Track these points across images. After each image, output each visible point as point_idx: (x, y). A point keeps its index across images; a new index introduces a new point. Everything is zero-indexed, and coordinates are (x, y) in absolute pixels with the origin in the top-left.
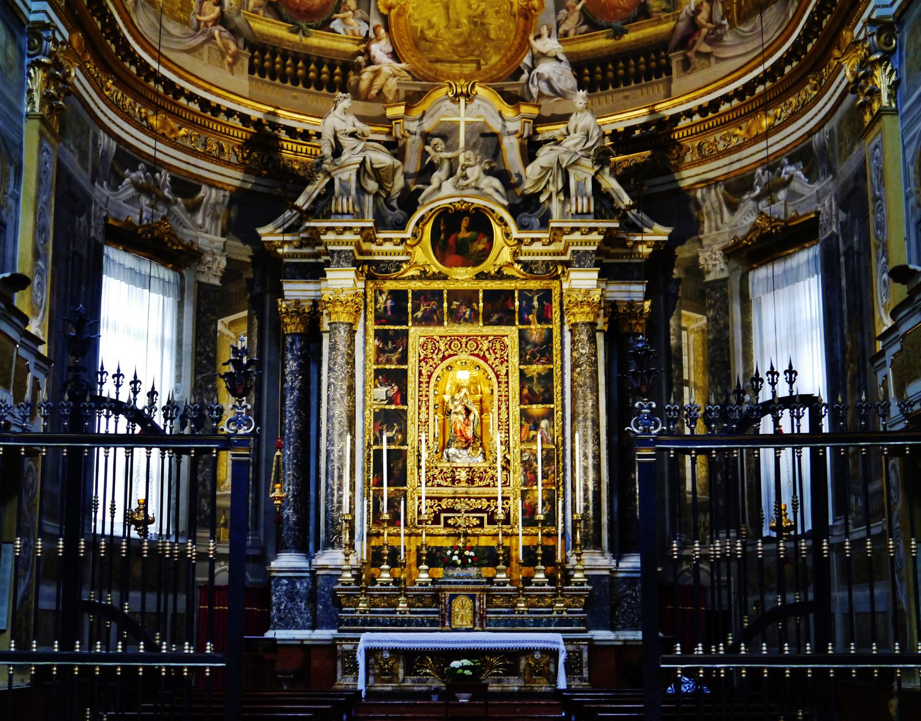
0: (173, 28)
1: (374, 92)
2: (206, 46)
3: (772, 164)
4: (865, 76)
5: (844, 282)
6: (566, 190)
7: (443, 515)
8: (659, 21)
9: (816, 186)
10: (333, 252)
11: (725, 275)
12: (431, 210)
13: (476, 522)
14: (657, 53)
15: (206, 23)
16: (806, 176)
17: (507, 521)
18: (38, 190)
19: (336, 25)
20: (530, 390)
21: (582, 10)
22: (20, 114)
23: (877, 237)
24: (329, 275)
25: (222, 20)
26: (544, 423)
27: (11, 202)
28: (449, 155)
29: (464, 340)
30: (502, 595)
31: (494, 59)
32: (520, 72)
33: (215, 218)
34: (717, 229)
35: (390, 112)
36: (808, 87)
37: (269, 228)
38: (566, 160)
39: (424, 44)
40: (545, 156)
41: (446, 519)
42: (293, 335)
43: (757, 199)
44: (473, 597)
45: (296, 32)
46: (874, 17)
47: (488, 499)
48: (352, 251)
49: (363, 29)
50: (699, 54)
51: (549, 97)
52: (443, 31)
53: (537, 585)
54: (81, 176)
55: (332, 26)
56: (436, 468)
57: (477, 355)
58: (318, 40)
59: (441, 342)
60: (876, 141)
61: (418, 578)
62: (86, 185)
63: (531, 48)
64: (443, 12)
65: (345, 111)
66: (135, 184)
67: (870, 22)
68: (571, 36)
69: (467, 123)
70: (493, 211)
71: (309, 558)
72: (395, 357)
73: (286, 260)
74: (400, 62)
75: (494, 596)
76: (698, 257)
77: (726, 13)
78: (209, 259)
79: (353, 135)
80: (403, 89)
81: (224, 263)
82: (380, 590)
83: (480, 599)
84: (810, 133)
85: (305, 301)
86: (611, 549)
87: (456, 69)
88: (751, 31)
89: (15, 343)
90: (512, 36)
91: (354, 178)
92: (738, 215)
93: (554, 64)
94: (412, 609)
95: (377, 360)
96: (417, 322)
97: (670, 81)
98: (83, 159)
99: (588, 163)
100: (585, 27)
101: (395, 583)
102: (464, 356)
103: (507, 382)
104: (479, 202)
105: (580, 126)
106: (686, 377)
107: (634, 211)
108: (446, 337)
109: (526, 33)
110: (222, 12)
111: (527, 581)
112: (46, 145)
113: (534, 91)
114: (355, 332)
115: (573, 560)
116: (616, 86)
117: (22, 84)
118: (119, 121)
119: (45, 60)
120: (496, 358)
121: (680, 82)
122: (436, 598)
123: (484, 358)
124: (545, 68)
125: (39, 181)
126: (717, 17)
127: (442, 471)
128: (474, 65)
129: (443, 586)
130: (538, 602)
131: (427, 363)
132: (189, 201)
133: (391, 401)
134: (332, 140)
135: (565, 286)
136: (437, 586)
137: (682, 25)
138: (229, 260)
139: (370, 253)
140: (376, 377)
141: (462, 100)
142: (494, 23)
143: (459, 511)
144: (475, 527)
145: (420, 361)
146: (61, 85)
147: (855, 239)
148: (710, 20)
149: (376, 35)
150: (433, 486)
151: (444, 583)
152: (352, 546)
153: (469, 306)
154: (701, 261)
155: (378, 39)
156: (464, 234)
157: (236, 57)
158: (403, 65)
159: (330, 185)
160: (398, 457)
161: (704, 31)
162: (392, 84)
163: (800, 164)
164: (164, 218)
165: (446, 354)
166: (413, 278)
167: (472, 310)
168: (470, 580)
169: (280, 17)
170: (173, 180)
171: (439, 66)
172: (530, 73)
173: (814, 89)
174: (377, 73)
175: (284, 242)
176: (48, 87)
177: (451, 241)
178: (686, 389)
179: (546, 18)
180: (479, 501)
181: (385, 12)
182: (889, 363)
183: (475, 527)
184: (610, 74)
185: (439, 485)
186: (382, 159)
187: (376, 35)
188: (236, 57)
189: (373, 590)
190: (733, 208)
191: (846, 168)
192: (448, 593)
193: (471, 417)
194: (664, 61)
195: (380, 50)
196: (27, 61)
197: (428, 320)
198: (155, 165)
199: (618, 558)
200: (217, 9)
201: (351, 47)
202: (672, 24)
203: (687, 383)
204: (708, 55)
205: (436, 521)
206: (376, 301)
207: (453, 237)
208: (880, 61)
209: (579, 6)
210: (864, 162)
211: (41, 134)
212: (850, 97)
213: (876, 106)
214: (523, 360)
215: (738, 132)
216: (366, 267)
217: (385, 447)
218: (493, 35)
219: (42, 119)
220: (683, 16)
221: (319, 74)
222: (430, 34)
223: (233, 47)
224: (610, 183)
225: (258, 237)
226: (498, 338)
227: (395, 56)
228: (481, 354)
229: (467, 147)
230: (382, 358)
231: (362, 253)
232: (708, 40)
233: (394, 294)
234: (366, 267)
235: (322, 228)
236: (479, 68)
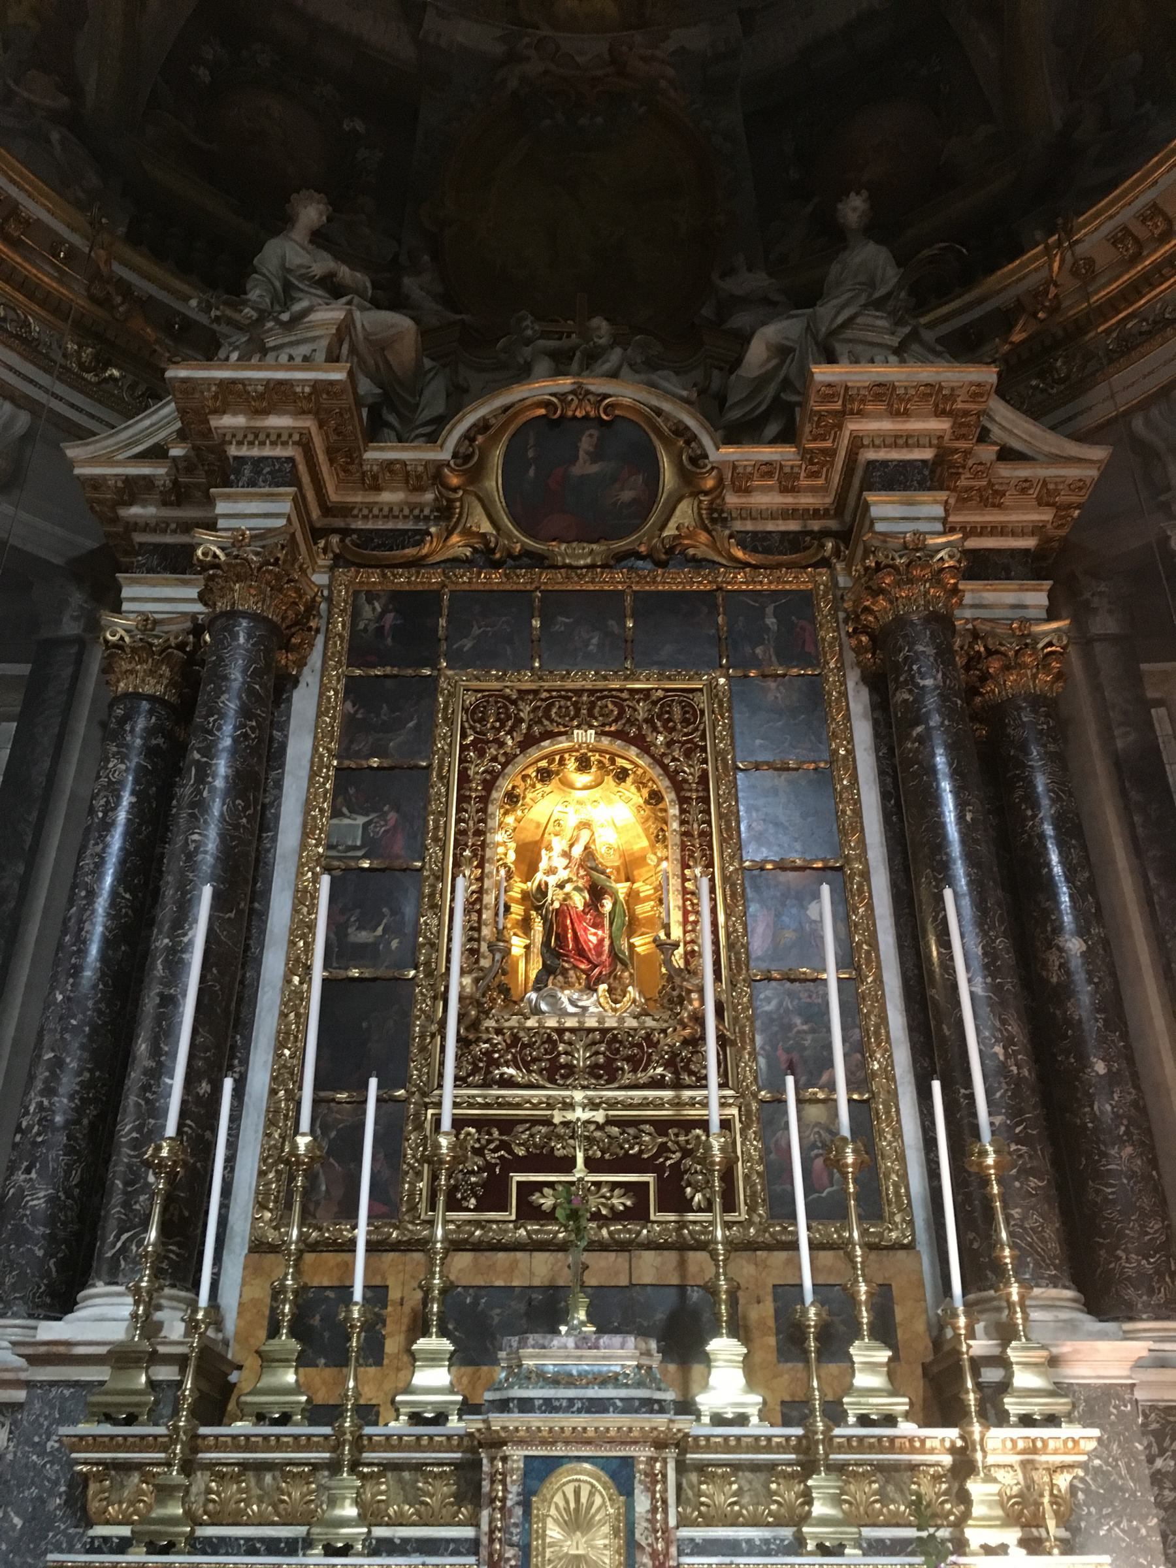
7: (518, 1177)
10: (241, 460)
12: (506, 409)
13: (620, 1202)
29: (585, 698)
30: (736, 1467)
47: (661, 1126)
48: (291, 460)
56: (499, 1031)
59: (521, 705)
61: (408, 1389)
70: (659, 412)
73: (139, 538)
75: (701, 1467)
76: (1169, 537)
82: (246, 1443)
83: (653, 1479)
85: (169, 621)
94: (380, 1532)
95: (348, 749)
102: (585, 736)
103: (706, 800)
108: (535, 692)
114: (296, 682)
120: (669, 744)
127: (516, 1039)
129: (499, 1421)
130: (884, 1499)
131: (481, 754)
134: (278, 284)
136: (473, 1424)
139: (345, 510)
140: (338, 790)
144: (617, 1216)
145: (463, 748)
150: (486, 1085)
151: (503, 1406)
156: (584, 467)
165: (536, 730)
166: (456, 561)
168: (609, 1393)
175: (134, 489)
180: (632, 1131)
183: (617, 1216)
189: (218, 1445)
192: (517, 1454)
193: (608, 905)
200: (64, 101)
205: (493, 1196)
206: (356, 614)
216: (335, 539)
228: (633, 731)
231: (327, 510)
233: (399, 600)
234: (335, 539)
235: (208, 381)
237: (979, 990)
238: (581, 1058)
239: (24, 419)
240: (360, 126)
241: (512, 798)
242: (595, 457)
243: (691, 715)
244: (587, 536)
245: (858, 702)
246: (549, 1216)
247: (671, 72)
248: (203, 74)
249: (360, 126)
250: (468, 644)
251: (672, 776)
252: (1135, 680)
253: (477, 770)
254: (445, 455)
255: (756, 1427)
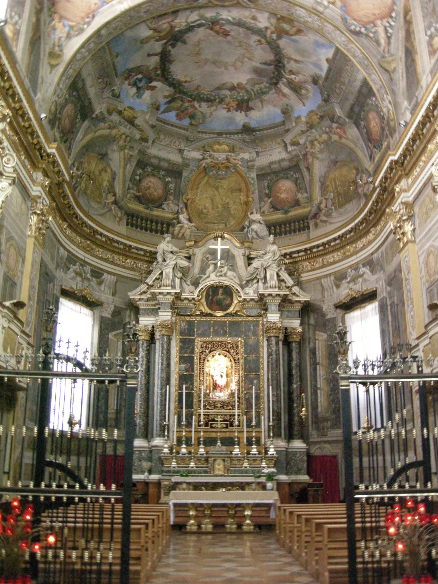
0: (94, 204)
1: (180, 235)
2: (108, 213)
3: (355, 267)
4: (400, 227)
5: (390, 318)
6: (265, 277)
7: (210, 423)
8: (304, 207)
9: (376, 277)
11: (335, 316)
13: (225, 426)
14: (303, 220)
15: (108, 203)
16: (371, 271)
17: (239, 426)
18: (32, 269)
19: (164, 206)
20: (249, 366)
21: (271, 202)
22: (25, 235)
23: (407, 296)
24: (160, 314)
25: (115, 202)
26: (255, 382)
27: (19, 274)
28: (214, 262)
31: (233, 222)
32: (244, 228)
33: (109, 288)
34: (331, 296)
35: (187, 244)
36: (371, 235)
37: (134, 292)
38: (265, 264)
39: (202, 216)
40: (256, 264)
41: (211, 424)
42: (143, 341)
43: (349, 282)
44: (224, 460)
45: (148, 209)
46: (403, 201)
47: (230, 415)
49: (176, 209)
50: (321, 221)
51: (257, 239)
52: (210, 210)
53: (253, 454)
54: (51, 266)
55: (163, 206)
57: (226, 350)
58: (156, 213)
60: (406, 254)
62: (53, 270)
63: (249, 218)
64: (211, 202)
65: (168, 242)
66: (75, 272)
67: (402, 203)
68: (266, 213)
69: (222, 249)
71: (149, 442)
72: (189, 351)
74: (191, 223)
77: (333, 204)
78: (106, 306)
79: (172, 252)
80: (193, 234)
81: (113, 308)
84: (372, 254)
86: (285, 438)
87: (216, 226)
88: (345, 210)
89: (17, 335)
90: (240, 213)
91: (171, 271)
92: (340, 289)
93: (259, 225)
96: (200, 335)
97: (309, 233)
98: (52, 259)
99: (274, 266)
100: (272, 209)
101: (206, 454)
104: (227, 283)
105: (272, 249)
106: (318, 361)
107: (296, 287)
109: (246, 211)
110: (115, 199)
111: (248, 453)
112: (36, 250)
113: (250, 236)
115: (269, 443)
116: (285, 234)
117: (27, 222)
118: (69, 243)
119: (38, 212)
121: (314, 233)
122: (207, 460)
123: (229, 352)
124: (255, 226)
125: (33, 265)
126: (329, 206)
128: (224, 225)
132: (98, 280)
133: (187, 370)
135: (265, 320)
137: (314, 209)
138: (115, 306)
140: (180, 360)
141: (219, 239)
142: (232, 207)
143: (217, 421)
146: (45, 224)
147: (395, 298)
148: (326, 207)
149: (182, 211)
152: (168, 437)
153: (222, 328)
154: (324, 309)
155: (183, 213)
156: (220, 296)
157: (121, 219)
158: (193, 224)
159: (161, 274)
160: (190, 396)
161: (324, 211)
162: (188, 232)
163: (368, 267)
164: (87, 287)
166: (197, 315)
167: (224, 330)
169: (141, 202)
170: (92, 271)
171: (209, 225)
172: (248, 228)
173: (374, 234)
174: (182, 227)
175: (140, 300)
176: (39, 224)
177: (214, 299)
178: (318, 366)
179: (255, 205)
181: (186, 201)
182: (421, 350)
184: (283, 230)
185: (208, 409)
186: (184, 263)
187: (182, 211)
188: (121, 219)
190: (338, 286)
191: (390, 268)
194: (306, 224)
195: (183, 217)
196: (30, 212)
197: (203, 335)
198: (83, 263)
199: (288, 442)
200: (114, 198)
201: (171, 216)
202: (310, 208)
203: (319, 364)
204: (325, 222)
207: (215, 297)
208: (407, 220)
209: (270, 201)
210: (400, 264)
211: (35, 244)
212: (392, 236)
213: (405, 239)
214: (245, 352)
215: (339, 253)
217: (184, 391)
218: (232, 212)
219: (36, 238)
220: (314, 205)
221: (157, 227)
222: (205, 211)
223: (120, 214)
224: (285, 275)
225: (128, 296)
226: (236, 343)
227: (190, 220)
229: (222, 258)
230: (183, 351)
232: (326, 215)
233: (188, 322)
236: (226, 226)
237: (274, 399)
238: (219, 405)
239: (115, 278)
240: (170, 179)
241: (208, 361)
242: (222, 294)
243: (238, 347)
244: (221, 310)
245: (266, 343)
246: (214, 428)
247: (240, 163)
248: (138, 178)
249: (170, 179)
250: (200, 332)
251: (234, 358)
252: (315, 334)
253: (203, 356)
254: (195, 297)
255: (239, 455)
